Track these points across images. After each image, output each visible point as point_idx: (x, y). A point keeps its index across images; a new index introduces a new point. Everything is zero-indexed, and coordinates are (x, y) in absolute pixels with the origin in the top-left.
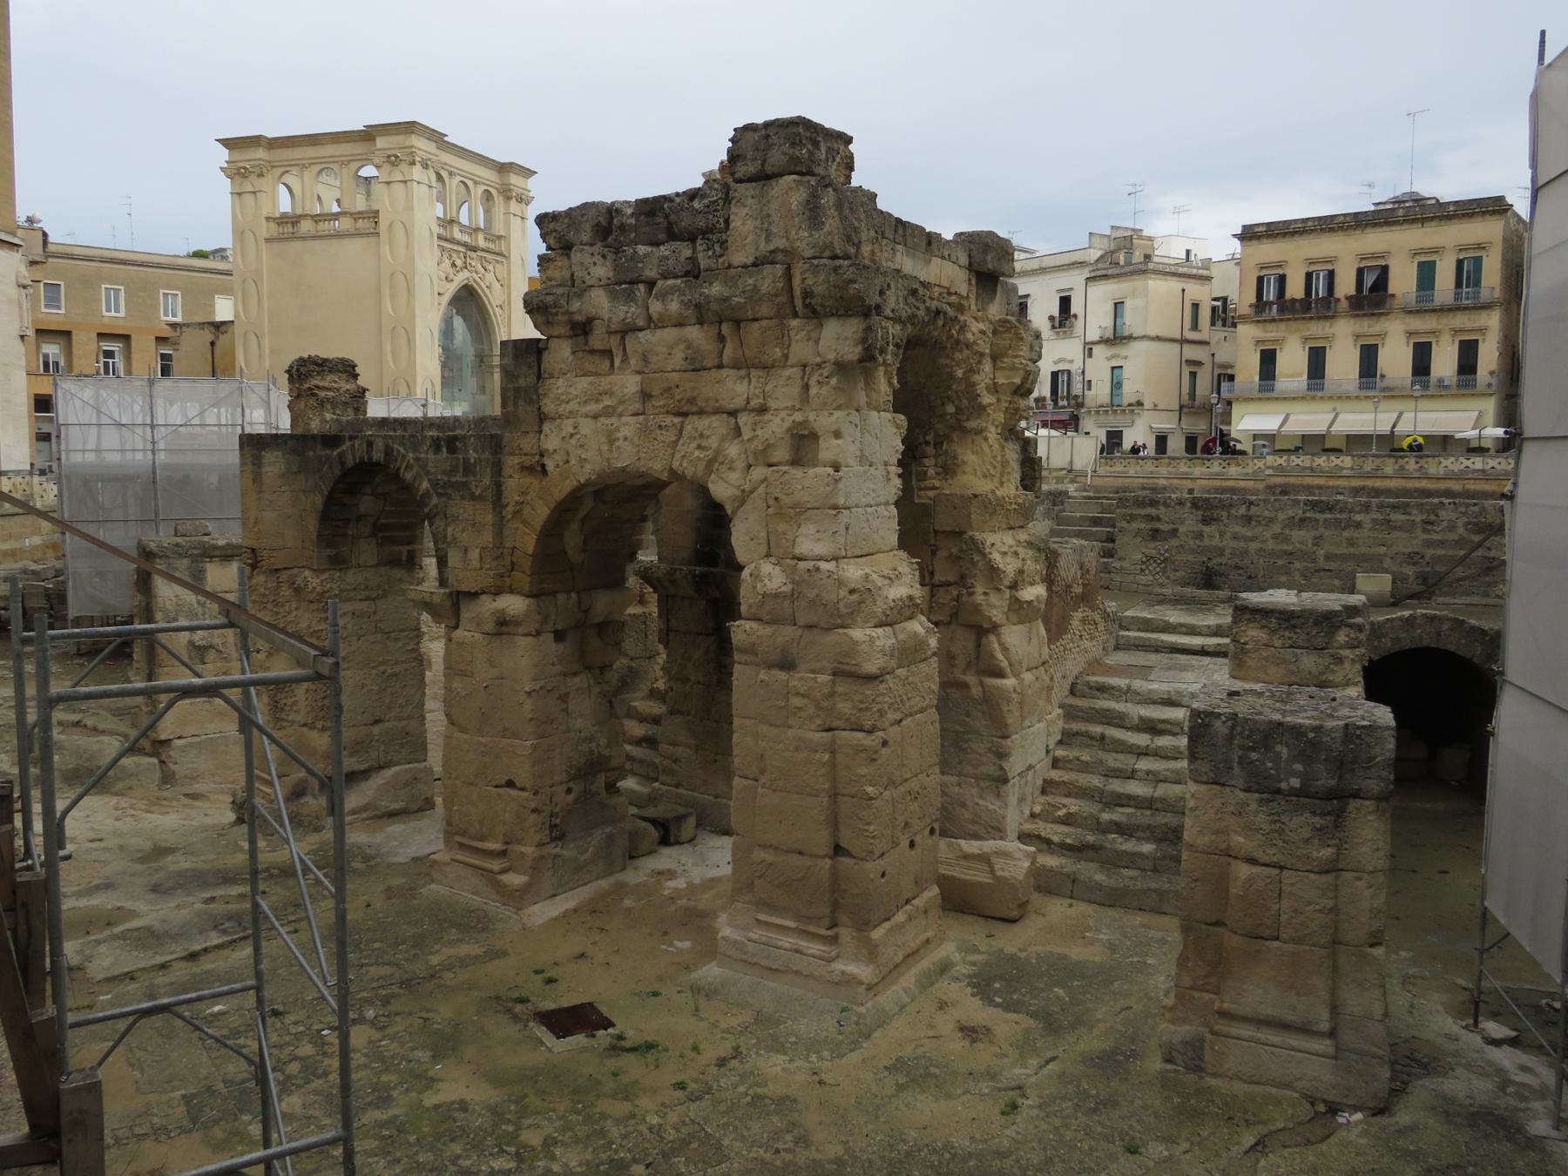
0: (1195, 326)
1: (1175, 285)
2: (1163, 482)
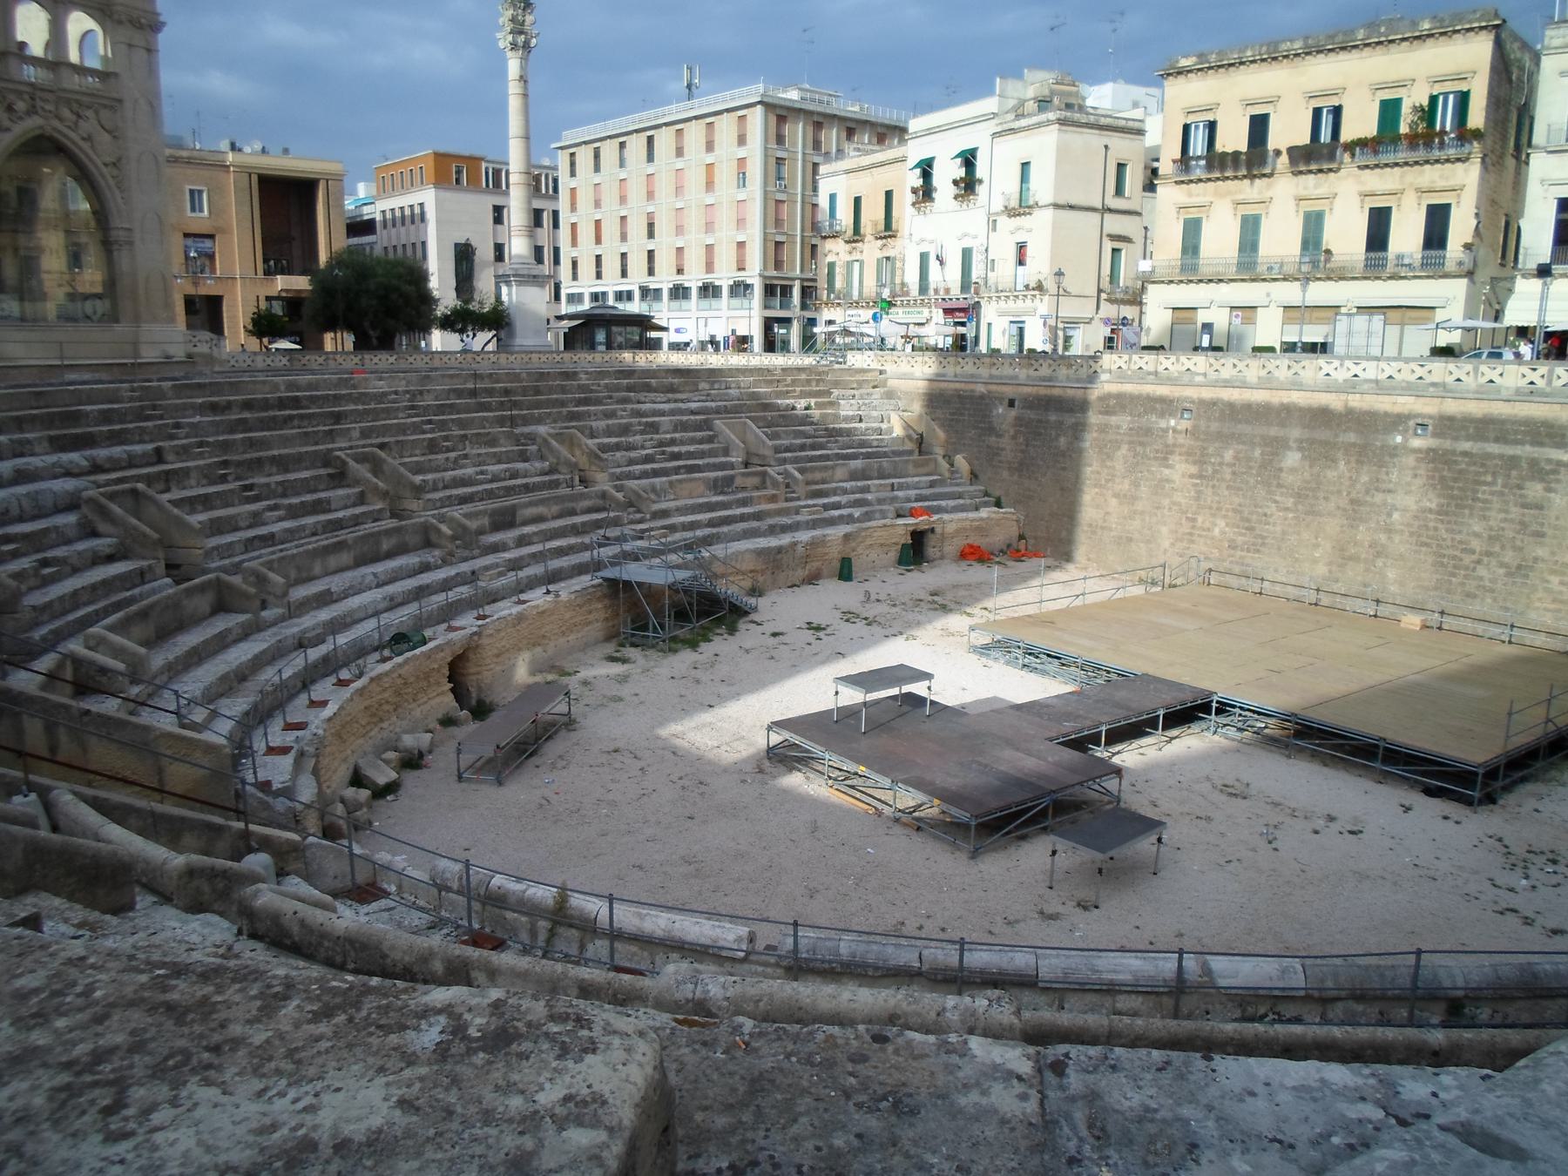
0: (1119, 191)
1: (1095, 140)
2: (981, 389)
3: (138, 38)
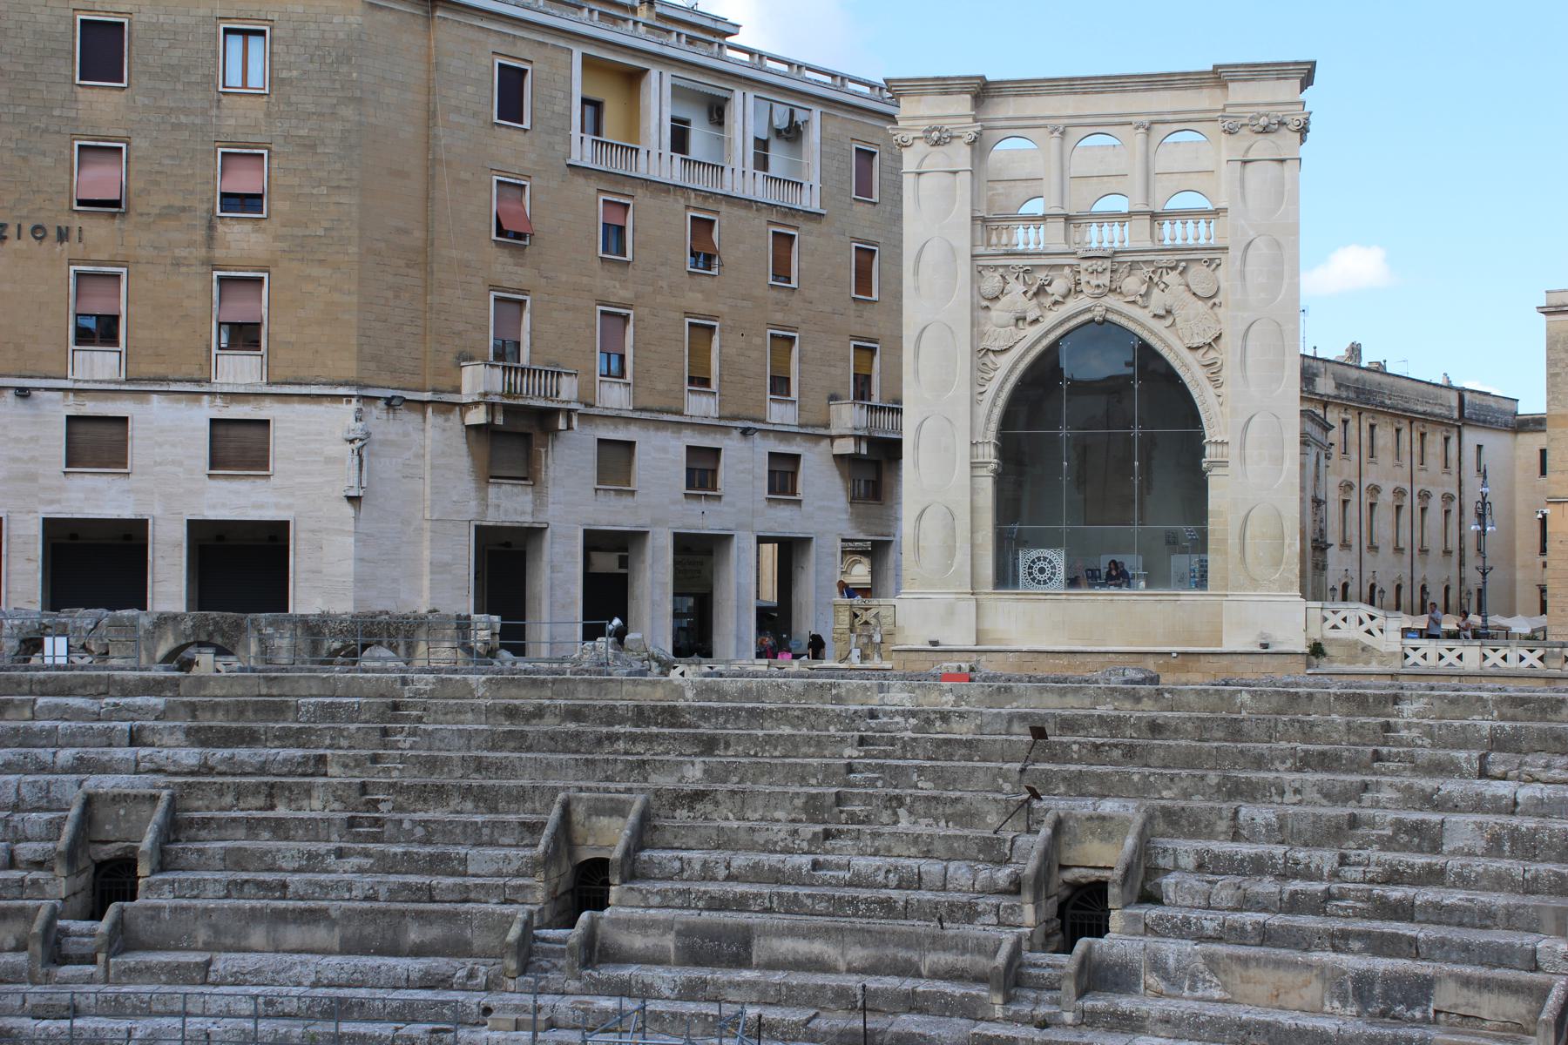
3: (1263, 147)
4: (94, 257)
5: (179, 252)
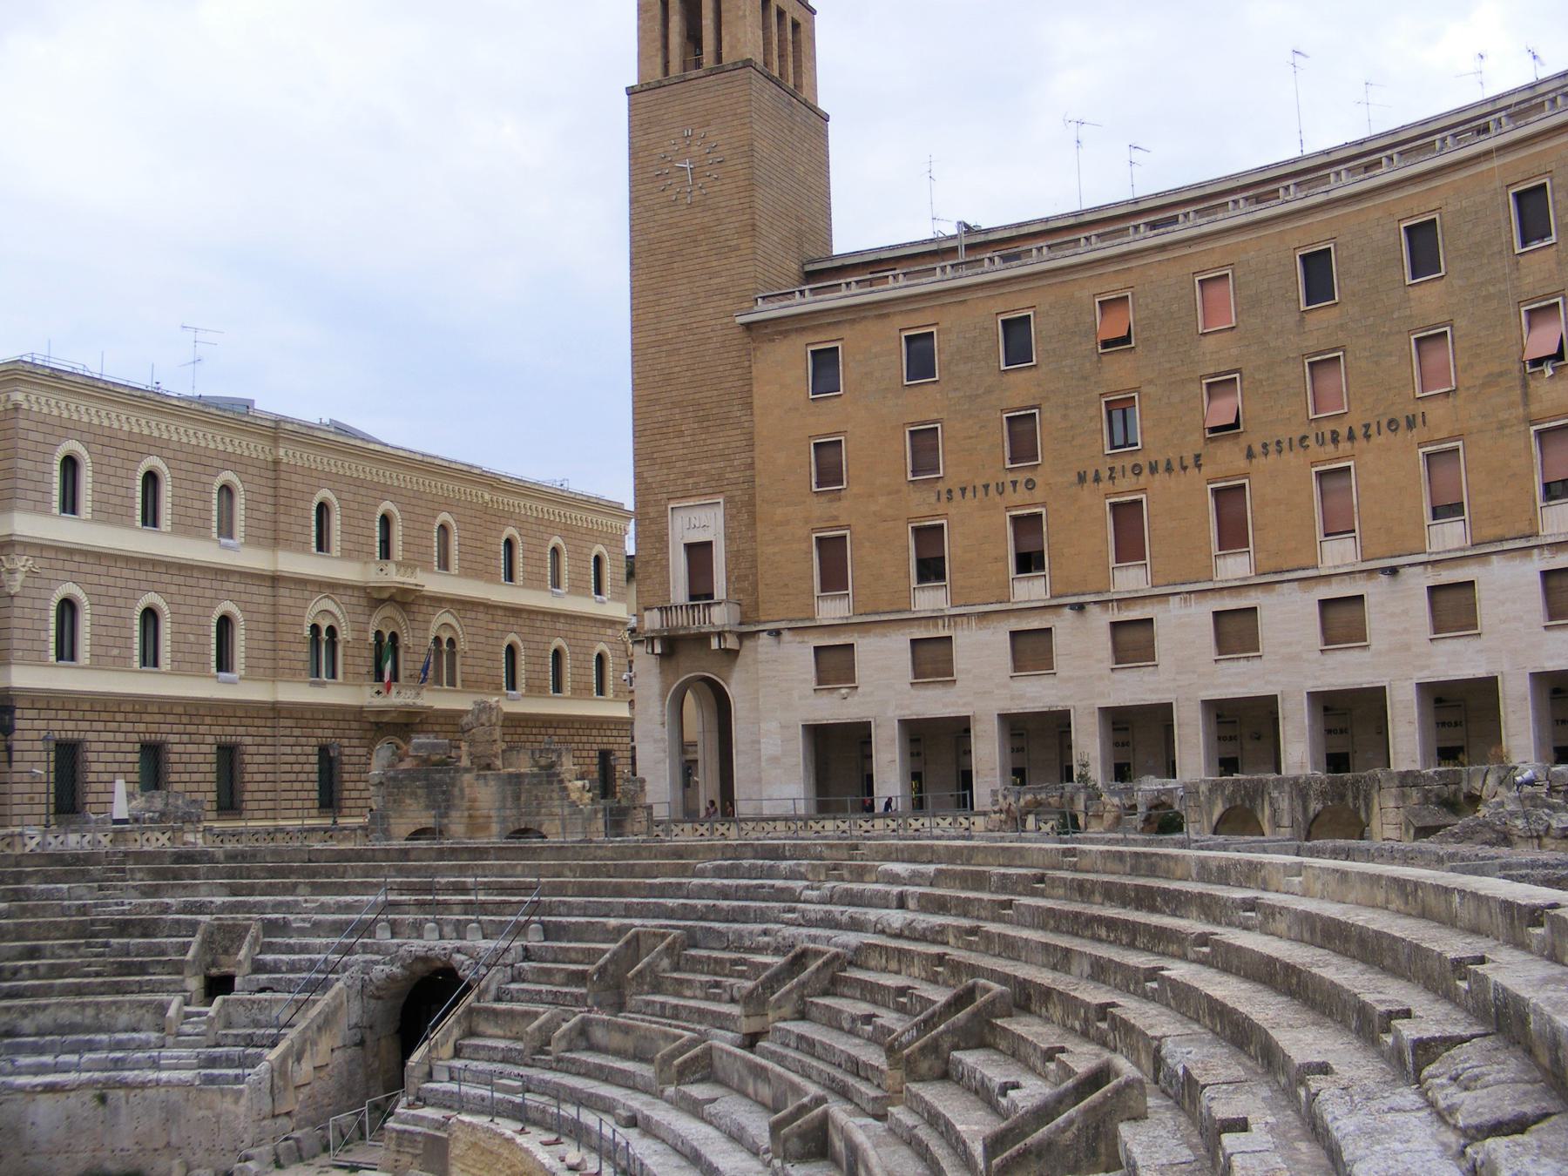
4: (1437, 437)
5: (1503, 416)
